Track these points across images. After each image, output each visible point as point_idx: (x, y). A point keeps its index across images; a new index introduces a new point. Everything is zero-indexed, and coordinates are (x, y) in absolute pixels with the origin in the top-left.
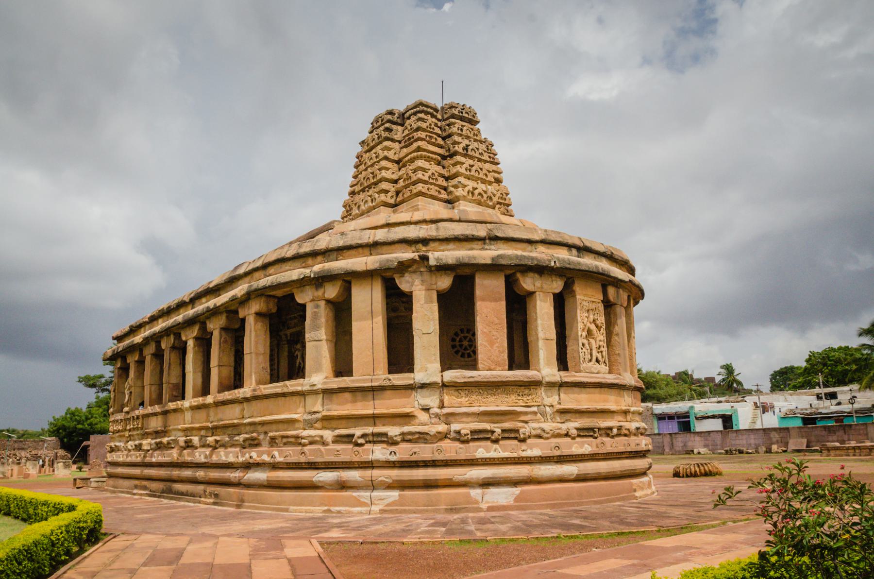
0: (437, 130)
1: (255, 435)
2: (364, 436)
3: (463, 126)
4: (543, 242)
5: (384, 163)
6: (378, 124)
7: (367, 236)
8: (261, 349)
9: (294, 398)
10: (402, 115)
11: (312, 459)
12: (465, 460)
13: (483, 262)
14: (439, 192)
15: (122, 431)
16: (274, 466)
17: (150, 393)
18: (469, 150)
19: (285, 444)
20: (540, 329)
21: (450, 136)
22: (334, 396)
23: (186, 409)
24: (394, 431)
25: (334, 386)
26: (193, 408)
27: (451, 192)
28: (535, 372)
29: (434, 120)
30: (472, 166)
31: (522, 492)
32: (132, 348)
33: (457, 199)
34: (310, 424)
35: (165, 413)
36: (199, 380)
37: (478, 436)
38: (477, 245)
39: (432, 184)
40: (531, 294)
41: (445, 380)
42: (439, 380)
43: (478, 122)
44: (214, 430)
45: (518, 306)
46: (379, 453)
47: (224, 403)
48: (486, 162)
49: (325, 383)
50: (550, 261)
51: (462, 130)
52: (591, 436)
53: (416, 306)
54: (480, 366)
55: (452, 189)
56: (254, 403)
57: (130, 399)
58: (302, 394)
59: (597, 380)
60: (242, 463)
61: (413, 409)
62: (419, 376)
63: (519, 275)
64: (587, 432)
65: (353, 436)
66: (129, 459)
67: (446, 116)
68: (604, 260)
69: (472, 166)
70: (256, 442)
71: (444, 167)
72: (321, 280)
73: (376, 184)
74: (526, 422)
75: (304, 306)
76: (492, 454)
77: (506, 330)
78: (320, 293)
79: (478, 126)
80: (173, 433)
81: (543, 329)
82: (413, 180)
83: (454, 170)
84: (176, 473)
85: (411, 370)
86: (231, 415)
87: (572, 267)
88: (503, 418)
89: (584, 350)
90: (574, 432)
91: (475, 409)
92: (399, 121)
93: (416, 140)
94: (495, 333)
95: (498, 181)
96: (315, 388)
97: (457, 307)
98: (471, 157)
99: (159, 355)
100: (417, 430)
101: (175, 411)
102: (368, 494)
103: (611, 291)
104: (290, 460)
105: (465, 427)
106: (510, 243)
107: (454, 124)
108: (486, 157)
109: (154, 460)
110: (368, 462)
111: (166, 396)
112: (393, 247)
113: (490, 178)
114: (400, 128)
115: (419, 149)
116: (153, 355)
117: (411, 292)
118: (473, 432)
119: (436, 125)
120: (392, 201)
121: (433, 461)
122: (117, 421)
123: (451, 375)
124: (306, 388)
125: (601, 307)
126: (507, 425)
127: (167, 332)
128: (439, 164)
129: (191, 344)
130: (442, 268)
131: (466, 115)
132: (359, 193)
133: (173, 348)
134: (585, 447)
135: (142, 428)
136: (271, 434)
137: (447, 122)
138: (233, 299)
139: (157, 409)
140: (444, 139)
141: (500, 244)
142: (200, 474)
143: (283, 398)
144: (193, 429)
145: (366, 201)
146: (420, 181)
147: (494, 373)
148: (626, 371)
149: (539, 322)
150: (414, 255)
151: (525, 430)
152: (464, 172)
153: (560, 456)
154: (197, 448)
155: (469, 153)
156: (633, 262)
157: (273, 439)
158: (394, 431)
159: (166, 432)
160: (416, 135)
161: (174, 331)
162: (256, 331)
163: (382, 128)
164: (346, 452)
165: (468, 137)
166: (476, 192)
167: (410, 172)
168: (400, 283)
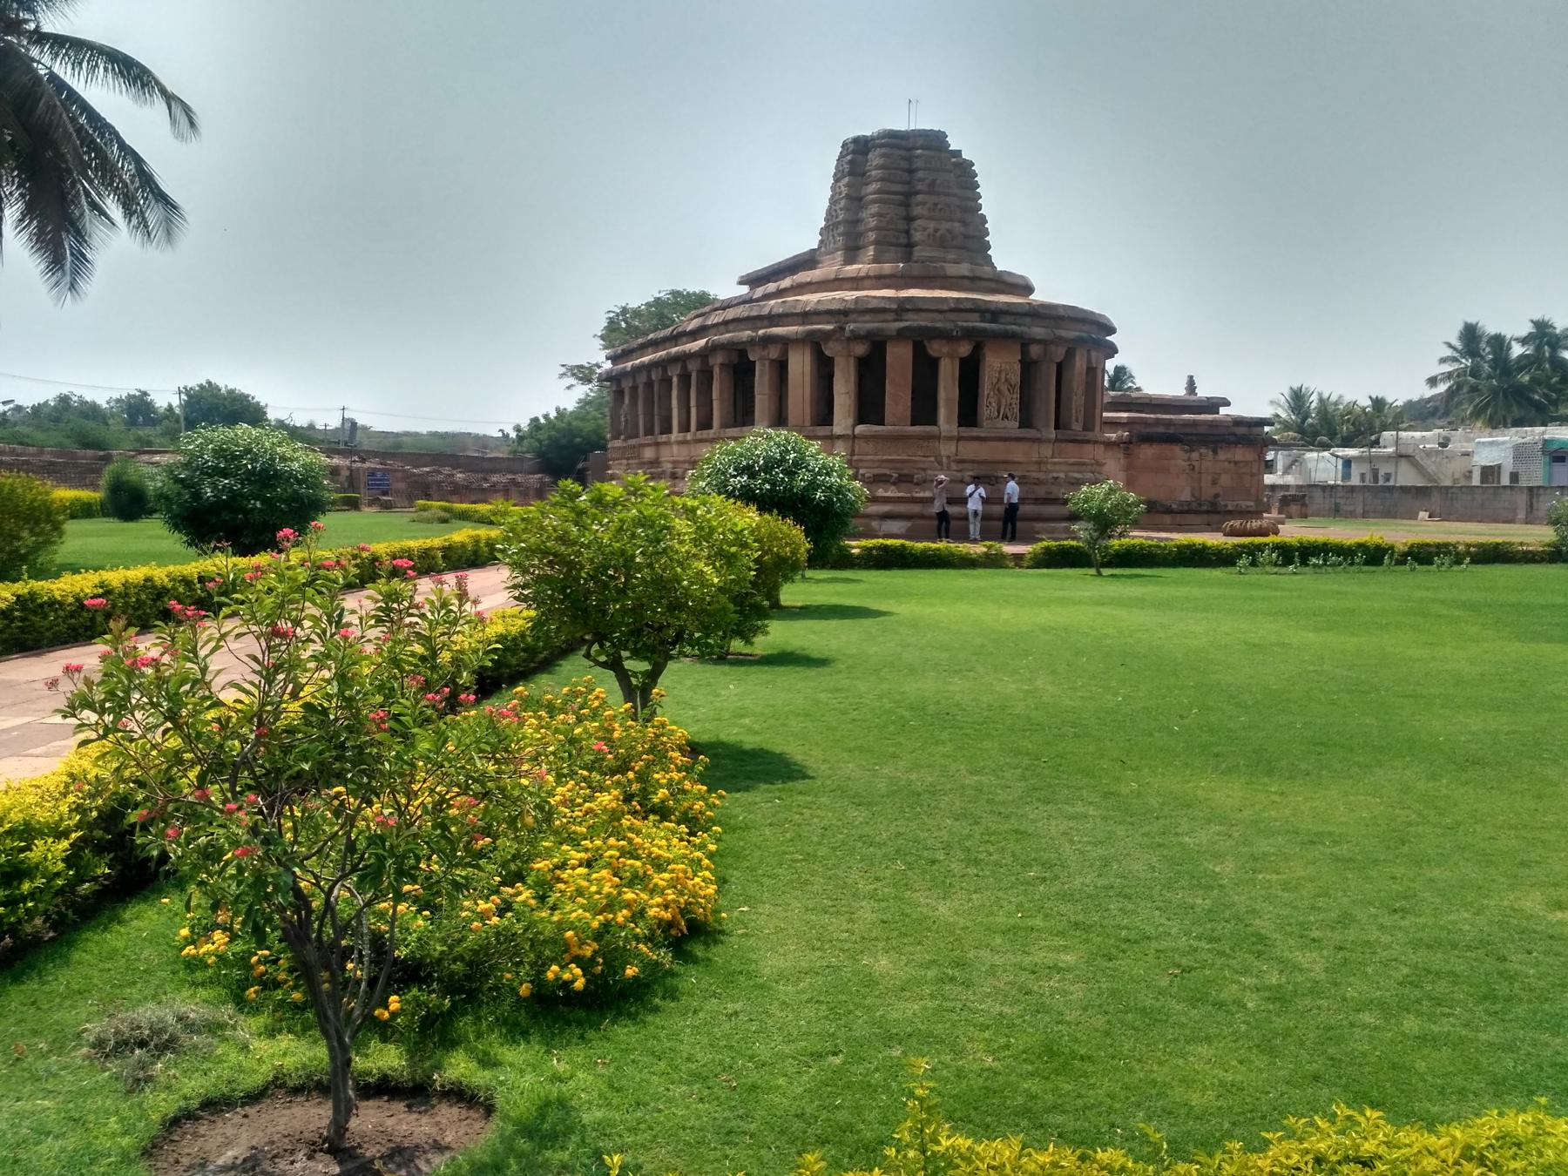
4: (952, 310)
21: (917, 170)
26: (680, 443)
28: (934, 428)
35: (657, 444)
38: (891, 316)
45: (926, 369)
72: (768, 340)
111: (657, 429)
123: (860, 429)
125: (1018, 367)
129: (675, 379)
130: (856, 337)
141: (910, 316)
151: (918, 477)
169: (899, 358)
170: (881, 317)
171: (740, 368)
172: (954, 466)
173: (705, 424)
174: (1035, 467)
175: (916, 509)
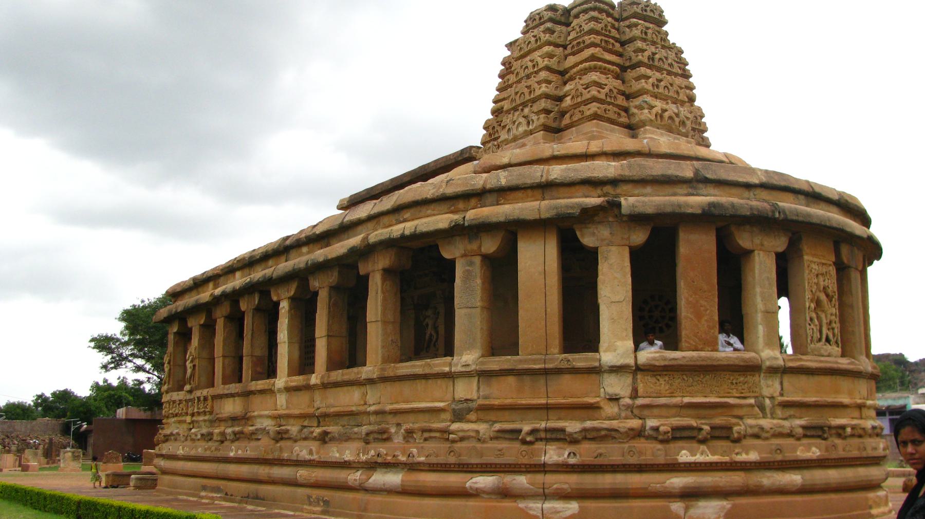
0: (614, 33)
1: (383, 425)
2: (533, 432)
3: (648, 28)
4: (763, 186)
5: (543, 75)
6: (535, 23)
7: (539, 174)
8: (390, 317)
9: (439, 381)
10: (567, 11)
11: (465, 459)
12: (663, 465)
13: (690, 211)
14: (619, 114)
15: (181, 415)
16: (412, 467)
17: (224, 368)
18: (656, 60)
19: (426, 440)
20: (759, 299)
21: (632, 40)
22: (494, 380)
23: (280, 391)
24: (573, 426)
25: (495, 367)
27: (633, 115)
28: (753, 354)
29: (610, 19)
30: (660, 81)
31: (734, 506)
32: (196, 309)
33: (643, 124)
34: (458, 416)
35: (247, 394)
36: (296, 354)
37: (681, 435)
38: (683, 189)
39: (609, 104)
40: (748, 253)
41: (639, 362)
42: (630, 361)
43: (665, 23)
44: (322, 418)
46: (552, 454)
47: (337, 385)
48: (676, 75)
49: (482, 363)
50: (773, 212)
51: (646, 34)
52: (819, 437)
53: (603, 268)
54: (684, 344)
55: (635, 111)
56: (381, 386)
57: (193, 375)
58: (450, 376)
59: (828, 365)
60: (366, 462)
61: (598, 399)
62: (607, 357)
63: (733, 228)
64: (816, 432)
65: (520, 431)
66: (193, 453)
67: (625, 15)
68: (835, 209)
69: (660, 81)
70: (385, 436)
71: (623, 82)
73: (534, 101)
74: (741, 418)
75: (452, 263)
76: (699, 458)
77: (716, 300)
78: (474, 246)
79: (665, 28)
80: (259, 420)
81: (763, 299)
82: (584, 98)
83: (636, 86)
84: (263, 471)
85: (596, 350)
86: (349, 399)
87: (801, 219)
88: (712, 412)
89: (812, 326)
90: (800, 431)
91: (676, 400)
92: (563, 19)
93: (588, 46)
94: (703, 302)
95: (692, 99)
96: (468, 369)
98: (659, 70)
99: (236, 319)
100: (604, 426)
101: (262, 392)
102: (539, 505)
103: (845, 250)
104: (433, 460)
105: (664, 424)
106: (727, 189)
107: (636, 25)
108: (676, 69)
109: (232, 454)
110: (540, 465)
111: (247, 372)
112: (573, 189)
113: (682, 97)
114: (564, 28)
115: (593, 58)
116: (226, 317)
117: (597, 248)
118: (675, 429)
119: (613, 27)
120: (554, 125)
121: (624, 465)
122: (174, 402)
124: (459, 369)
125: (833, 271)
126: (718, 421)
127: (248, 289)
128: (617, 77)
129: (284, 306)
130: (638, 219)
131: (652, 14)
132: (508, 112)
133: (257, 310)
134: (813, 451)
135: (211, 413)
136: (409, 426)
137: (627, 23)
138: (353, 251)
139: (234, 388)
140: (623, 44)
141: (711, 190)
142: (302, 473)
143: (423, 381)
144: (288, 416)
145: (520, 123)
146: (594, 99)
147: (703, 354)
148: (861, 354)
149: (758, 290)
151: (738, 429)
152: (651, 88)
153: (782, 461)
154: (296, 441)
155: (656, 63)
156: (871, 213)
157: (409, 433)
158: (573, 426)
159: (248, 419)
160: (588, 39)
161: (263, 288)
162: (383, 292)
163: (542, 28)
165: (654, 43)
166: (666, 114)
167: (580, 88)
168: (582, 236)
169: (696, 253)
170: (669, 189)
172: (779, 412)
173: (351, 353)
174: (856, 413)
175: (736, 479)
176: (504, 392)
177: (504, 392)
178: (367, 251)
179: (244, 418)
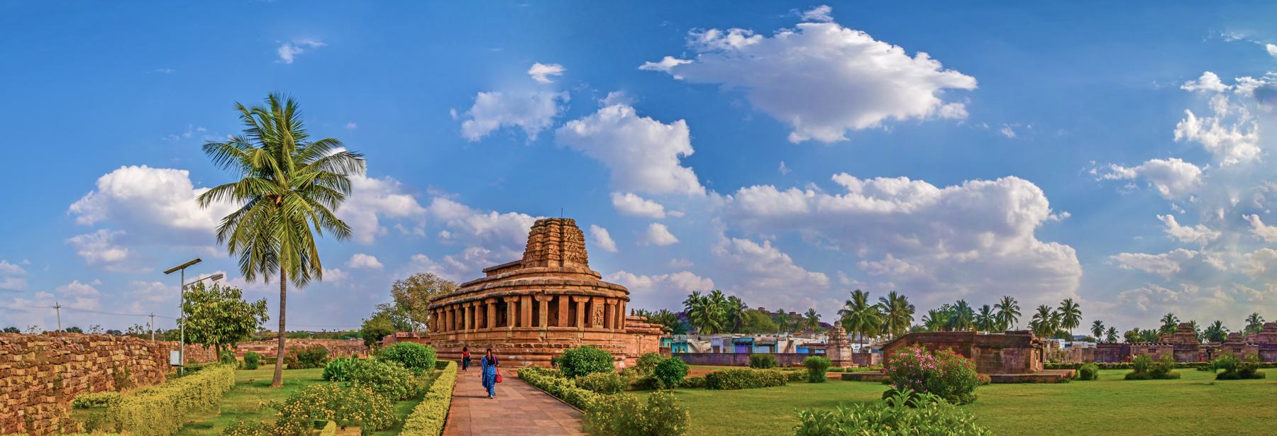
32: (440, 307)
44: (477, 341)
72: (512, 295)
86: (483, 336)
97: (554, 304)
99: (453, 311)
130: (549, 295)
150: (540, 290)
161: (461, 304)
164: (517, 350)
169: (564, 302)
171: (501, 305)
176: (518, 335)
177: (518, 335)
178: (487, 298)
179: (456, 341)
